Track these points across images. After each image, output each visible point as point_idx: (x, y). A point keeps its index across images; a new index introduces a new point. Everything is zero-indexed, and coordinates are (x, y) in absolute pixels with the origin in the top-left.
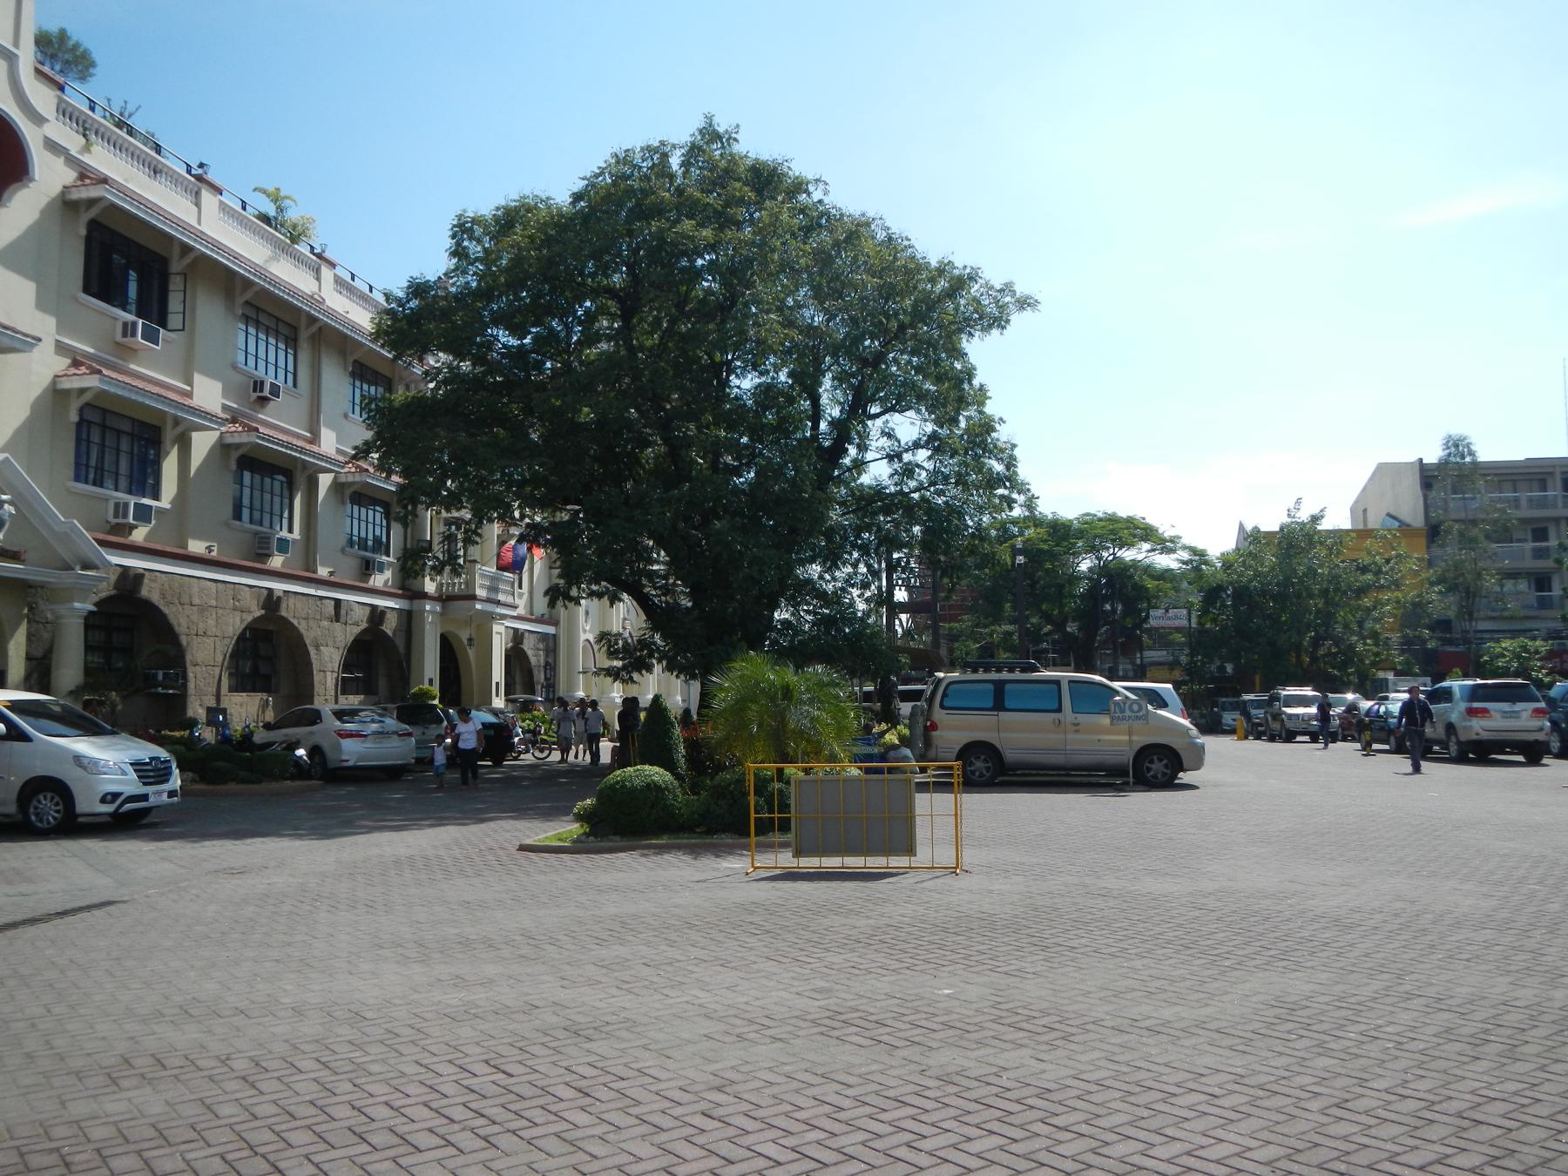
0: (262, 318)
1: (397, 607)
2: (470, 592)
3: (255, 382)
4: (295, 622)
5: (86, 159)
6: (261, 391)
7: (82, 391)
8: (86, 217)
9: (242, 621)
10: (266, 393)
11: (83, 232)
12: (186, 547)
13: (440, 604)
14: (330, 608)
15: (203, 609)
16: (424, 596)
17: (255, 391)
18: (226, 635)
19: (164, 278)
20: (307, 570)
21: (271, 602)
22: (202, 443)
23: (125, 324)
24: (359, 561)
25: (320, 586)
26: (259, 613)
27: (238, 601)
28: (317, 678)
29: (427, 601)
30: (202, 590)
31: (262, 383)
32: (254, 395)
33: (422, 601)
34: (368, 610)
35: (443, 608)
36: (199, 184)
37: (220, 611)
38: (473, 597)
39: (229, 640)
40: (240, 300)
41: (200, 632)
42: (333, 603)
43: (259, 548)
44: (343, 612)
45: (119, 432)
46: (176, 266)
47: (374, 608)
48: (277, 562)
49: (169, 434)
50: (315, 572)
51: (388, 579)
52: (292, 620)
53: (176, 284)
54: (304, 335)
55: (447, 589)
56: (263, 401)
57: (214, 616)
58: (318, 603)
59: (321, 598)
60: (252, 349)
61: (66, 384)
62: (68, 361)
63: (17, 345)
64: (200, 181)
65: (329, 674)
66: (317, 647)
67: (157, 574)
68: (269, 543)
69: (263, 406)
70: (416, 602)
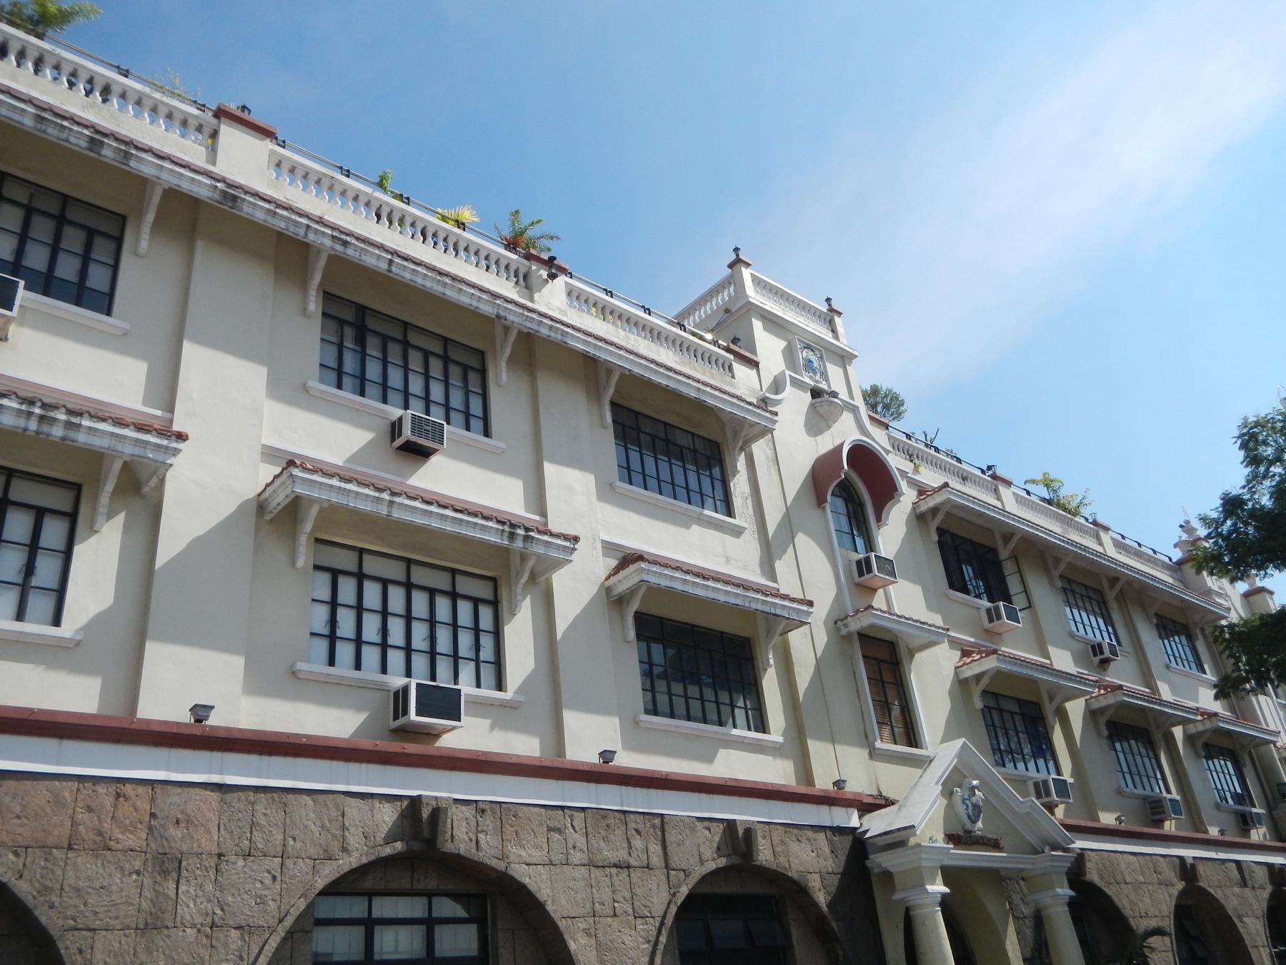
0: (1075, 588)
3: (1093, 647)
4: (1212, 891)
5: (917, 477)
6: (1102, 653)
7: (978, 677)
8: (934, 525)
10: (1107, 654)
11: (935, 538)
12: (1098, 820)
15: (1137, 886)
17: (1095, 655)
19: (997, 564)
20: (1197, 831)
21: (1187, 871)
22: (1076, 709)
23: (988, 611)
26: (1181, 885)
27: (1160, 873)
28: (1254, 955)
31: (1100, 645)
32: (1096, 660)
36: (996, 482)
39: (1168, 919)
40: (1056, 574)
41: (1143, 914)
43: (1154, 814)
45: (1012, 713)
46: (1004, 553)
48: (1169, 827)
49: (1049, 709)
52: (1208, 889)
53: (1009, 568)
54: (1111, 596)
56: (1105, 663)
59: (1224, 861)
60: (1078, 618)
61: (968, 673)
62: (959, 653)
63: (934, 638)
64: (997, 480)
65: (1261, 949)
66: (1240, 918)
68: (1162, 806)
69: (1105, 669)
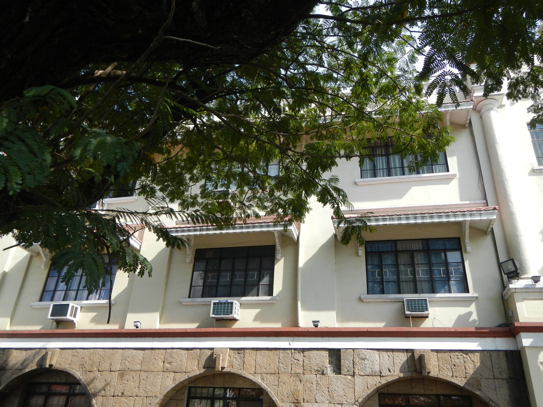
9: (174, 380)
14: (325, 359)
18: (150, 394)
25: (295, 338)
27: (170, 363)
29: (522, 334)
30: (124, 358)
37: (142, 373)
42: (326, 354)
44: (346, 363)
57: (137, 378)
58: (299, 356)
59: (303, 350)
67: (79, 350)
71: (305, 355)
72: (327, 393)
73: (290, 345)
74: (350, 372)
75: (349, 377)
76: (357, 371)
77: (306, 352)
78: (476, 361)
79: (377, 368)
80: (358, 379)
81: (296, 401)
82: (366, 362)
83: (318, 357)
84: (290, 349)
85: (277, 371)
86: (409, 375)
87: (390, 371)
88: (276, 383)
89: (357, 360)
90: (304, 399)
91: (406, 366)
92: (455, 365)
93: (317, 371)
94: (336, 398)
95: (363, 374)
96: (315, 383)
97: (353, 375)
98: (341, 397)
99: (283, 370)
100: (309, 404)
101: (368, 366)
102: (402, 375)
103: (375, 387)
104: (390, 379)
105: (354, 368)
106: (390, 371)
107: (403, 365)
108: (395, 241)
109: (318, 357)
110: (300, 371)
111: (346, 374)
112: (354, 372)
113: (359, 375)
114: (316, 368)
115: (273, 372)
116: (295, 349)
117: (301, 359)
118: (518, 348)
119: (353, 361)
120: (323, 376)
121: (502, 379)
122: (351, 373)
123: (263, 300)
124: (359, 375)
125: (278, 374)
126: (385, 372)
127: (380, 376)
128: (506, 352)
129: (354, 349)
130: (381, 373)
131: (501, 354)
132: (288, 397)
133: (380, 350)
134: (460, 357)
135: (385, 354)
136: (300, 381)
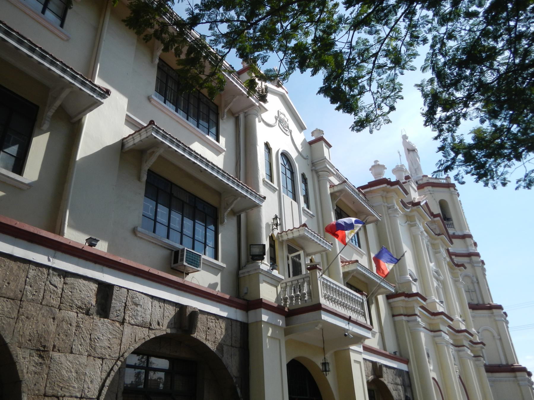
1: (225, 314)
2: (314, 302)
13: (284, 317)
16: (259, 304)
24: (166, 252)
25: (59, 254)
29: (263, 310)
33: (258, 310)
34: (171, 312)
35: (287, 323)
38: (318, 307)
42: (94, 287)
44: (116, 304)
47: (182, 308)
50: (61, 233)
51: (216, 284)
55: (291, 303)
58: (58, 281)
59: (65, 274)
70: (252, 313)
71: (67, 282)
72: (88, 341)
73: (49, 260)
74: (119, 317)
75: (118, 324)
76: (127, 318)
77: (69, 279)
78: (223, 327)
79: (148, 319)
80: (127, 329)
81: (42, 349)
82: (139, 308)
83: (84, 289)
84: (48, 267)
85: (20, 296)
86: (174, 331)
87: (159, 324)
88: (15, 315)
89: (129, 303)
90: (54, 346)
91: (173, 322)
92: (209, 329)
93: (80, 308)
94: (99, 350)
95: (133, 323)
96: (74, 324)
97: (122, 323)
98: (105, 348)
99: (30, 297)
100: (60, 354)
101: (140, 314)
102: (169, 331)
103: (143, 341)
104: (159, 333)
105: (124, 313)
106: (159, 324)
107: (171, 320)
108: (172, 184)
109: (84, 289)
110: (55, 302)
111: (114, 319)
112: (124, 319)
113: (129, 323)
114: (79, 304)
115: (12, 295)
116: (54, 269)
117: (60, 286)
118: (248, 321)
119: (125, 303)
120: (87, 317)
121: (236, 347)
122: (120, 318)
123: (8, 177)
124: (129, 323)
125: (21, 301)
126: (155, 325)
127: (149, 329)
128: (241, 323)
129: (128, 290)
130: (151, 325)
131: (238, 324)
132: (30, 340)
133: (154, 298)
134: (213, 321)
135: (156, 303)
136: (54, 319)
